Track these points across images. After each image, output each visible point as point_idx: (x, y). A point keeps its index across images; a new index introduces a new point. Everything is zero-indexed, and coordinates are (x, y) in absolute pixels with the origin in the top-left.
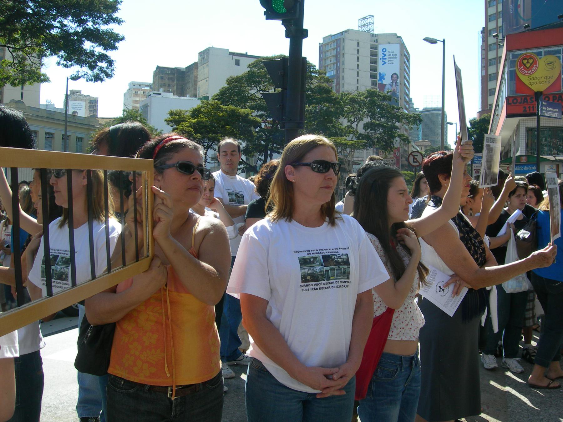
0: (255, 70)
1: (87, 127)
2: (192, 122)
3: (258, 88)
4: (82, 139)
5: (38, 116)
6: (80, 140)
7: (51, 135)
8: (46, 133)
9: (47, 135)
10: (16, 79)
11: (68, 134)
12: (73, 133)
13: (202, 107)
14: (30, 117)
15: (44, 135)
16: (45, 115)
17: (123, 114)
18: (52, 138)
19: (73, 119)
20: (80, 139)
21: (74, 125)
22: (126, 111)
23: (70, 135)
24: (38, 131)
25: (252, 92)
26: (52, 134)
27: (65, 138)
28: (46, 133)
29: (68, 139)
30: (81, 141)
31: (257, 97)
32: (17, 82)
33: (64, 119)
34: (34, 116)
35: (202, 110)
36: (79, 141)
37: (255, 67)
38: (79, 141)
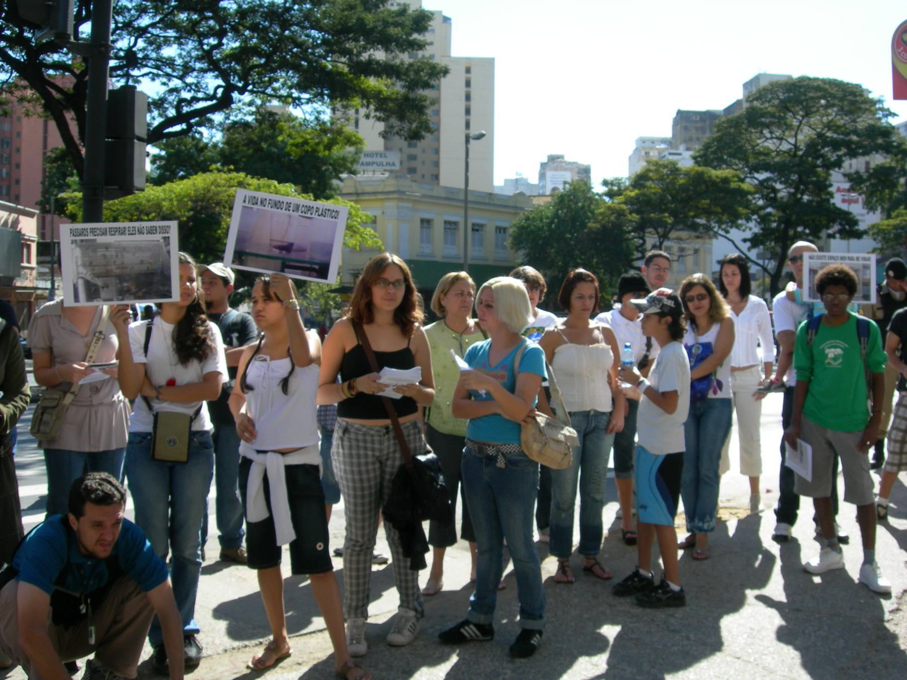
0: (756, 104)
1: (512, 211)
2: (629, 196)
3: (768, 135)
5: (431, 197)
6: (502, 231)
8: (446, 222)
11: (471, 221)
13: (648, 170)
14: (417, 199)
15: (442, 225)
16: (443, 195)
17: (564, 188)
19: (490, 199)
20: (501, 230)
21: (492, 208)
22: (569, 183)
23: (482, 226)
24: (433, 220)
25: (759, 141)
26: (456, 223)
28: (446, 222)
29: (482, 230)
30: (505, 232)
31: (771, 150)
33: (462, 197)
34: (424, 196)
35: (651, 174)
36: (500, 232)
37: (757, 99)
38: (500, 232)
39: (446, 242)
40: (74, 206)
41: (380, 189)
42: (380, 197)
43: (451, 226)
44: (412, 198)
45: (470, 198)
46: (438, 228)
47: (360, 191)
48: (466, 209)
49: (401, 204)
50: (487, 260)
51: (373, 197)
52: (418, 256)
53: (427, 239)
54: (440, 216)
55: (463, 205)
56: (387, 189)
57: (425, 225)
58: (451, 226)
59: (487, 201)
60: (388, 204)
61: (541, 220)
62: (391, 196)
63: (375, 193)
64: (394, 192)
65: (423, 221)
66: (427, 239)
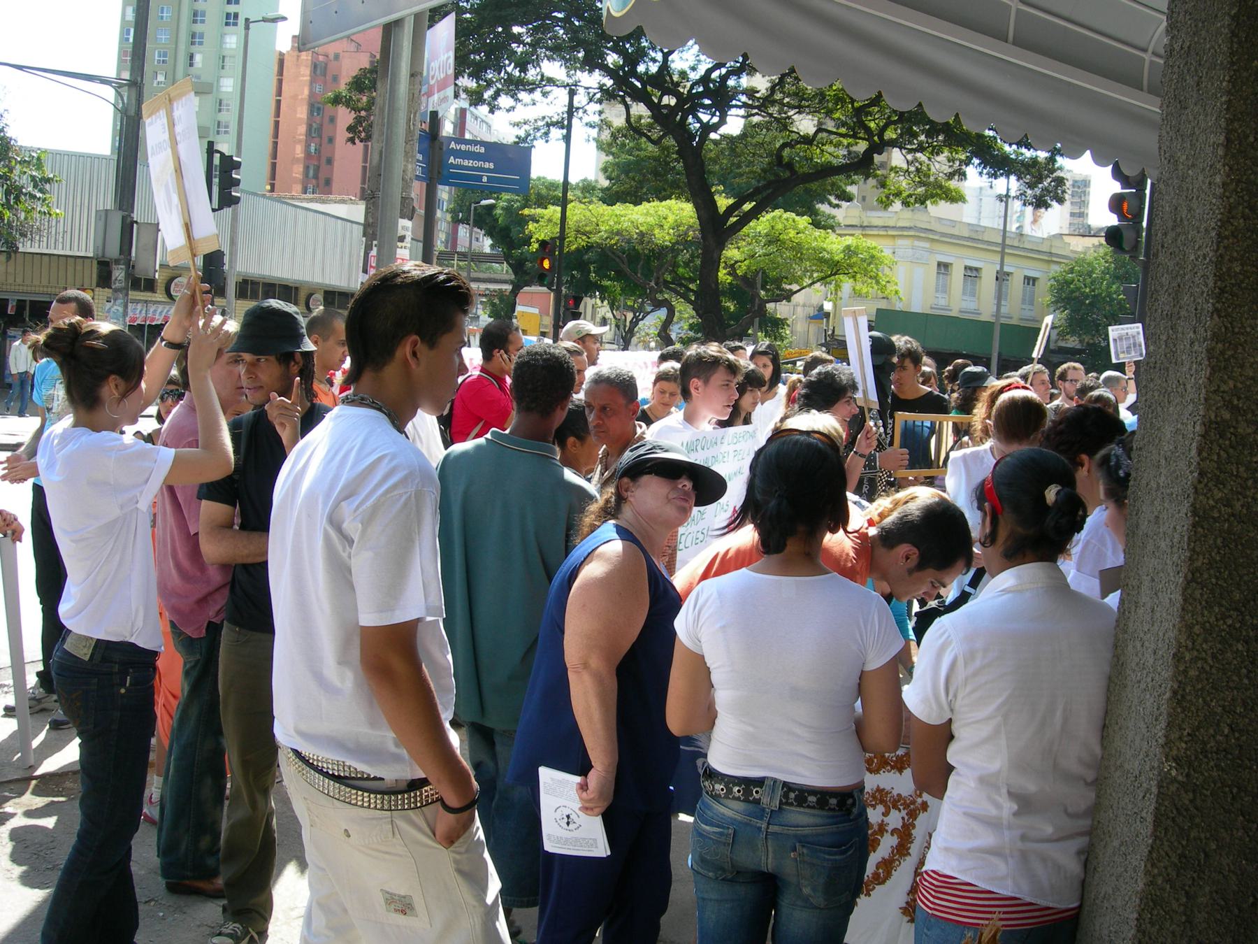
1: (1046, 258)
4: (1034, 280)
5: (952, 236)
6: (1031, 283)
7: (975, 272)
9: (969, 271)
10: (910, 196)
11: (1006, 269)
12: (1018, 269)
15: (962, 271)
18: (976, 277)
19: (1019, 241)
20: (1030, 281)
23: (1012, 273)
24: (951, 264)
26: (977, 270)
27: (1002, 277)
29: (1008, 280)
30: (1034, 285)
32: (912, 200)
33: (1000, 241)
36: (1028, 284)
38: (1028, 284)
39: (964, 293)
40: (535, 224)
41: (891, 223)
42: (890, 233)
43: (972, 273)
44: (931, 236)
45: (1008, 242)
46: (957, 273)
47: (865, 224)
48: (1003, 254)
49: (917, 243)
50: (1011, 318)
51: (882, 233)
52: (961, 312)
53: (944, 289)
54: (960, 260)
55: (999, 249)
56: (900, 224)
57: (942, 268)
58: (972, 273)
59: (1016, 244)
60: (900, 242)
61: (1090, 274)
62: (905, 233)
63: (885, 227)
64: (911, 228)
65: (939, 264)
66: (944, 289)
